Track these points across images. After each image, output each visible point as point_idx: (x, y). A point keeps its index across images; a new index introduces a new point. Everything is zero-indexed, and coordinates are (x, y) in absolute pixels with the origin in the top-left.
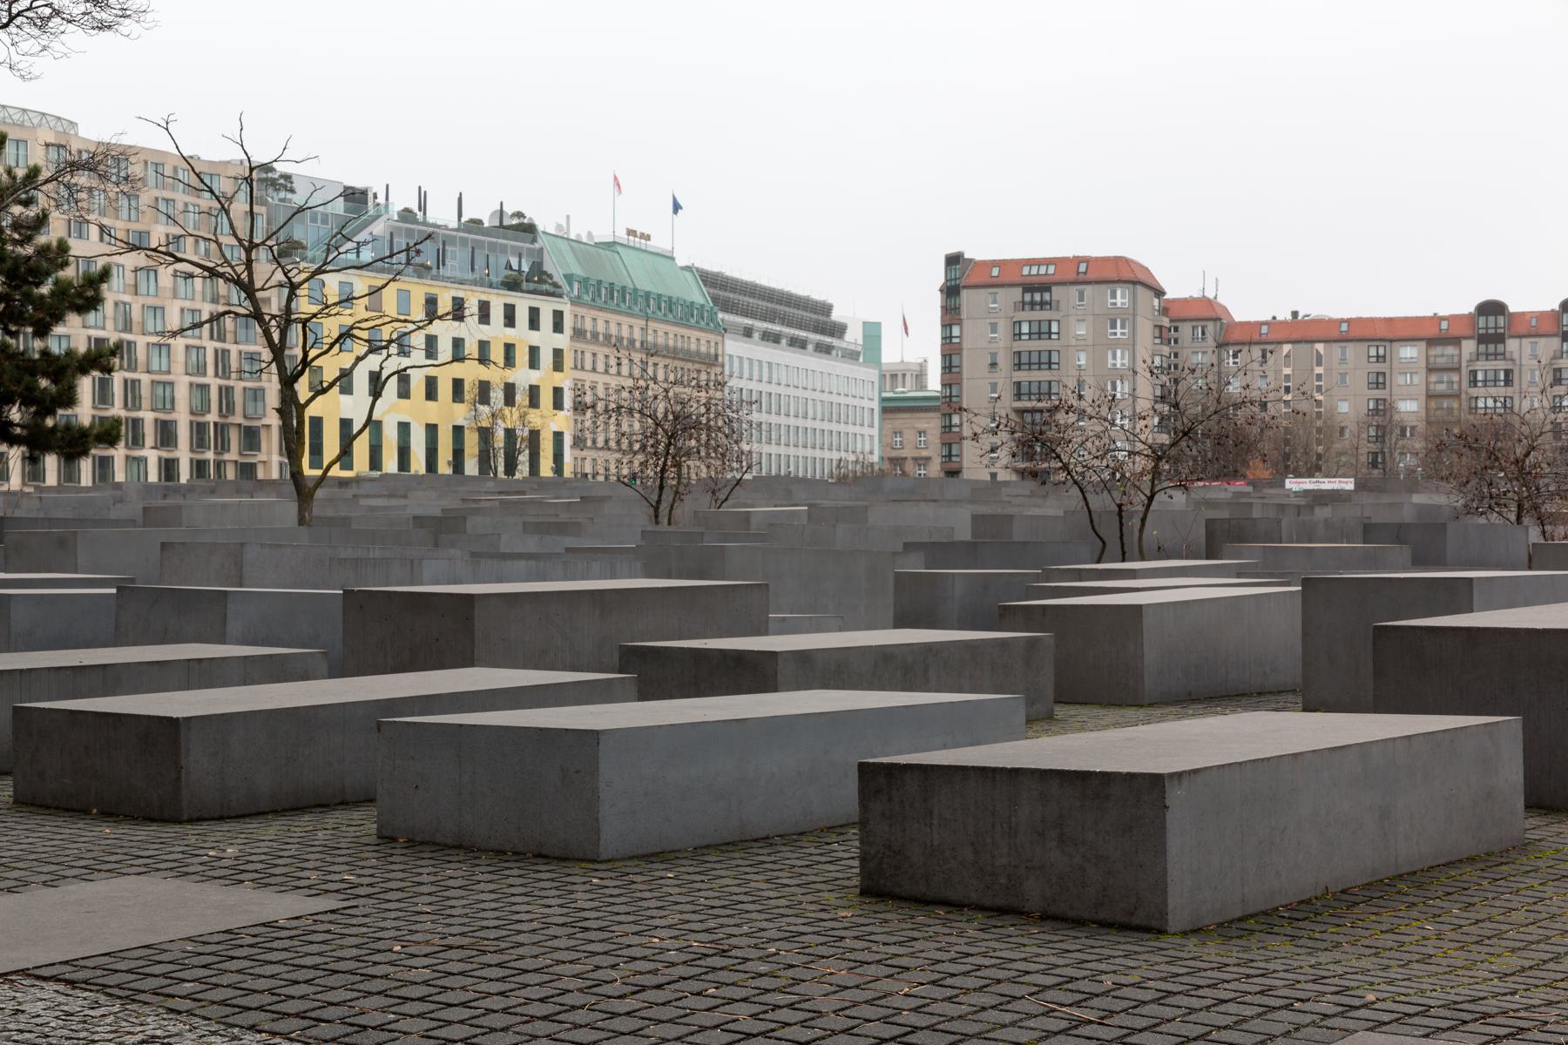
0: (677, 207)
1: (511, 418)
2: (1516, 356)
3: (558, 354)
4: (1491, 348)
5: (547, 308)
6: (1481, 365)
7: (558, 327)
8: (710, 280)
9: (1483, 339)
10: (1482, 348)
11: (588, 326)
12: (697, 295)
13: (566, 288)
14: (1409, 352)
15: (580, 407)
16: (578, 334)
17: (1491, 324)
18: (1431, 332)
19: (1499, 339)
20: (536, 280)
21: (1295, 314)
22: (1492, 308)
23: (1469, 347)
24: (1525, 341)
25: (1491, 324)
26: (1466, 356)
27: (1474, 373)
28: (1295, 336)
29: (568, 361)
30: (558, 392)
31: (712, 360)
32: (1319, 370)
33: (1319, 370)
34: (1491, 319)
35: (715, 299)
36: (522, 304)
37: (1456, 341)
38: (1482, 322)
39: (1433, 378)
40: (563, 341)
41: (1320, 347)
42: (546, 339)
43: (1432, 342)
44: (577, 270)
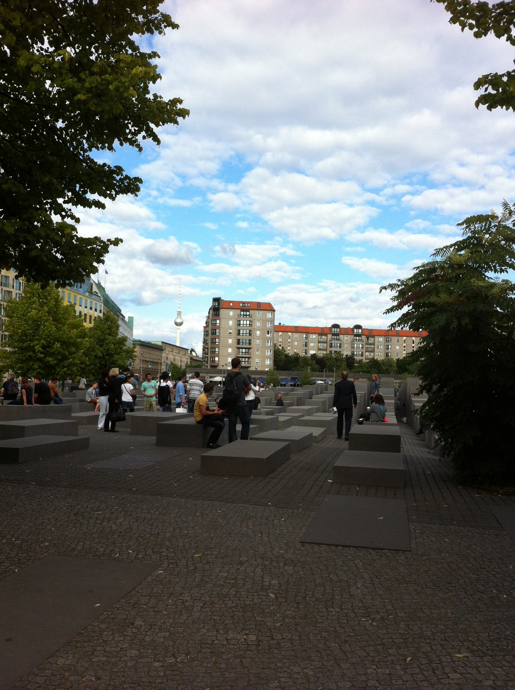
2: (342, 340)
4: (335, 337)
6: (333, 342)
9: (334, 335)
10: (333, 337)
14: (314, 336)
17: (336, 330)
18: (320, 332)
19: (337, 335)
21: (280, 324)
22: (336, 326)
23: (330, 336)
24: (345, 336)
25: (336, 330)
26: (329, 339)
27: (332, 344)
28: (284, 330)
32: (289, 340)
33: (289, 340)
34: (336, 329)
37: (326, 335)
38: (333, 329)
39: (320, 344)
41: (290, 334)
43: (321, 334)
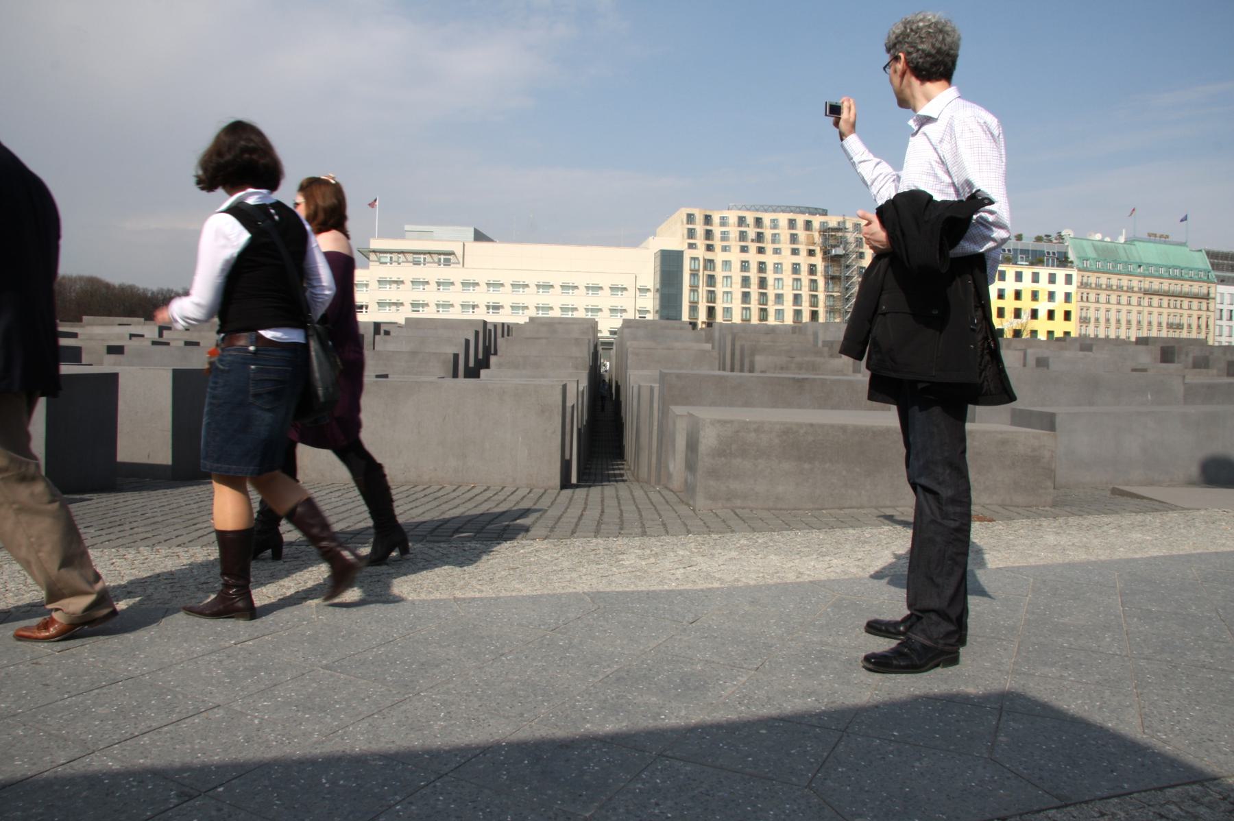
0: (1184, 219)
1: (1016, 324)
3: (1068, 297)
5: (1061, 273)
7: (1069, 279)
8: (1211, 255)
11: (1093, 279)
12: (1205, 263)
13: (1076, 262)
15: (1084, 321)
16: (1083, 285)
20: (1063, 261)
29: (1074, 298)
30: (1067, 315)
31: (1207, 297)
35: (1213, 265)
36: (1044, 272)
40: (1072, 289)
42: (1060, 288)
44: (1091, 254)
